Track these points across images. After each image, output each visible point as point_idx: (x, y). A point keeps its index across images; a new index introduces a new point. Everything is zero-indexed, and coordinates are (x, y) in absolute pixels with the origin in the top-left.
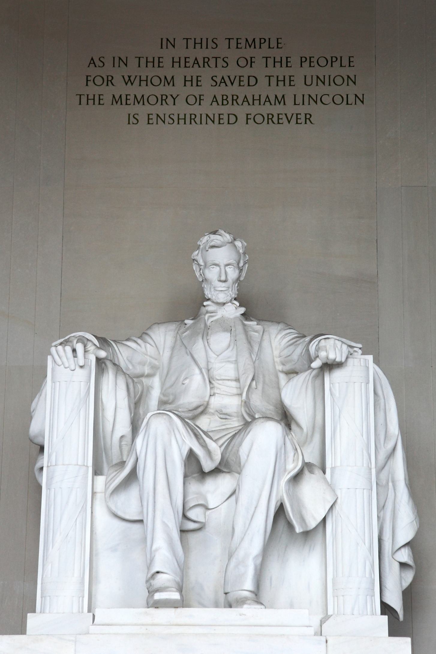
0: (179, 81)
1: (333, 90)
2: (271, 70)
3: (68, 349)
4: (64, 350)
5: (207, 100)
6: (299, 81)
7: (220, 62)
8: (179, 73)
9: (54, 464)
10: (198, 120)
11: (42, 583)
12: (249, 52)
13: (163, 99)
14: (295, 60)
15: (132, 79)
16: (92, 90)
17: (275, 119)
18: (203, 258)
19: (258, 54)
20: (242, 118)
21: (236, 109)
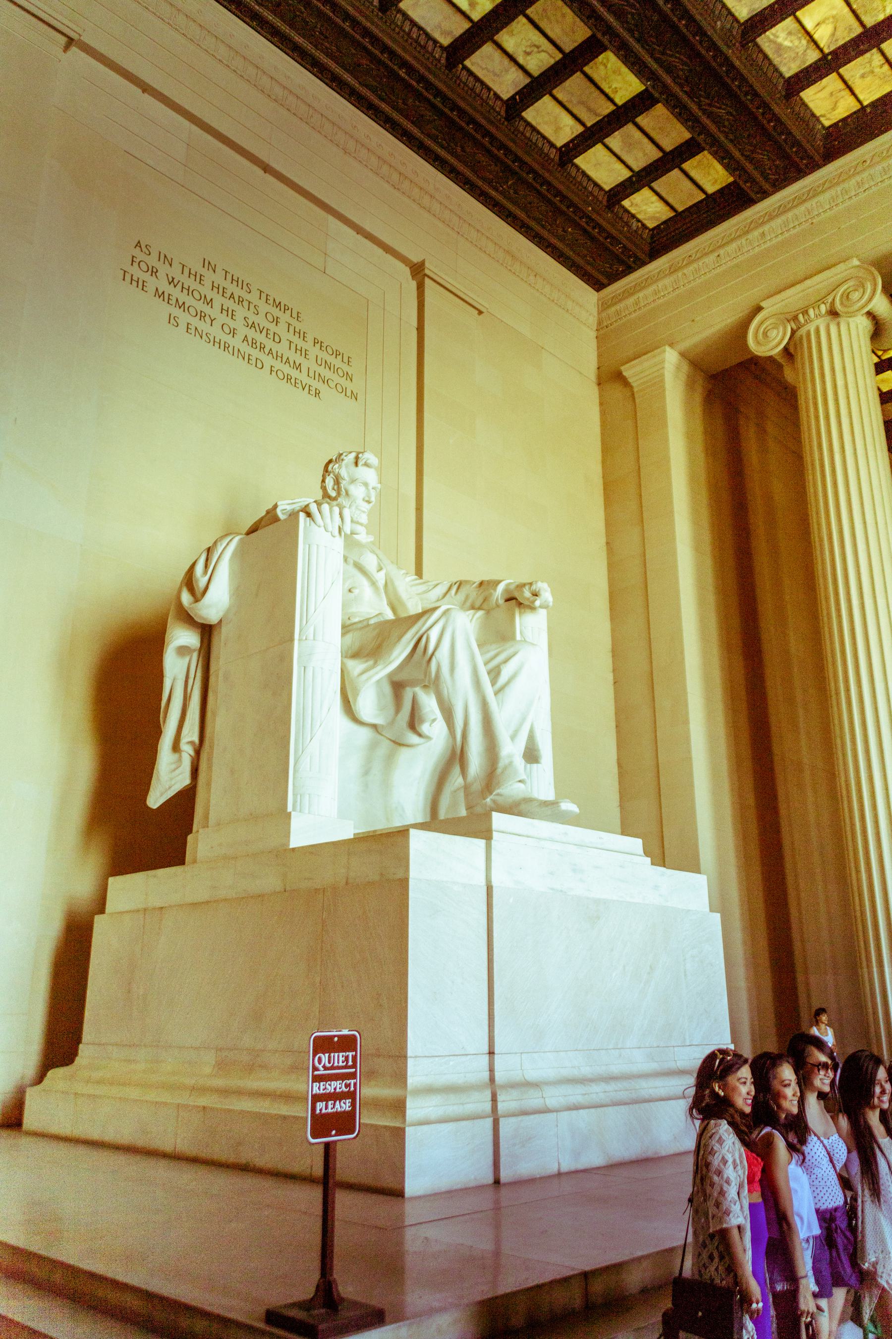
0: (217, 304)
1: (335, 377)
2: (290, 336)
3: (336, 510)
4: (331, 511)
5: (240, 337)
6: (312, 356)
7: (252, 306)
8: (218, 300)
9: (311, 637)
10: (231, 349)
11: (294, 778)
12: (276, 312)
13: (202, 316)
14: (310, 338)
15: (176, 281)
16: (135, 271)
17: (293, 381)
18: (348, 473)
19: (285, 317)
20: (267, 368)
21: (262, 356)
